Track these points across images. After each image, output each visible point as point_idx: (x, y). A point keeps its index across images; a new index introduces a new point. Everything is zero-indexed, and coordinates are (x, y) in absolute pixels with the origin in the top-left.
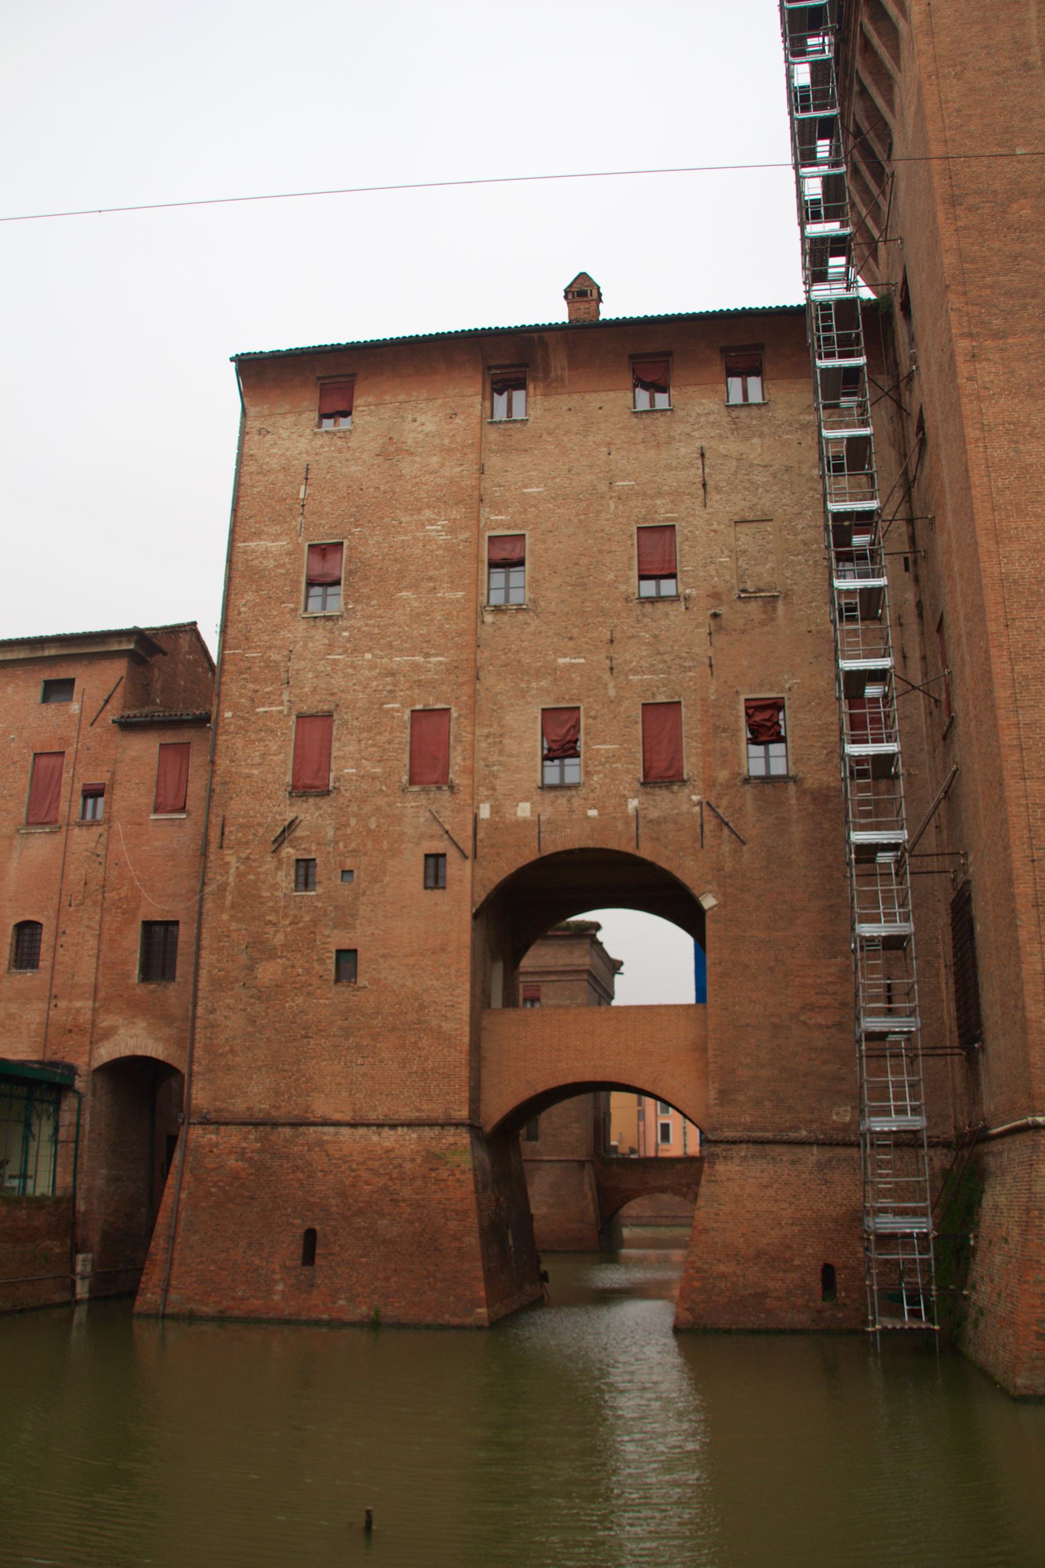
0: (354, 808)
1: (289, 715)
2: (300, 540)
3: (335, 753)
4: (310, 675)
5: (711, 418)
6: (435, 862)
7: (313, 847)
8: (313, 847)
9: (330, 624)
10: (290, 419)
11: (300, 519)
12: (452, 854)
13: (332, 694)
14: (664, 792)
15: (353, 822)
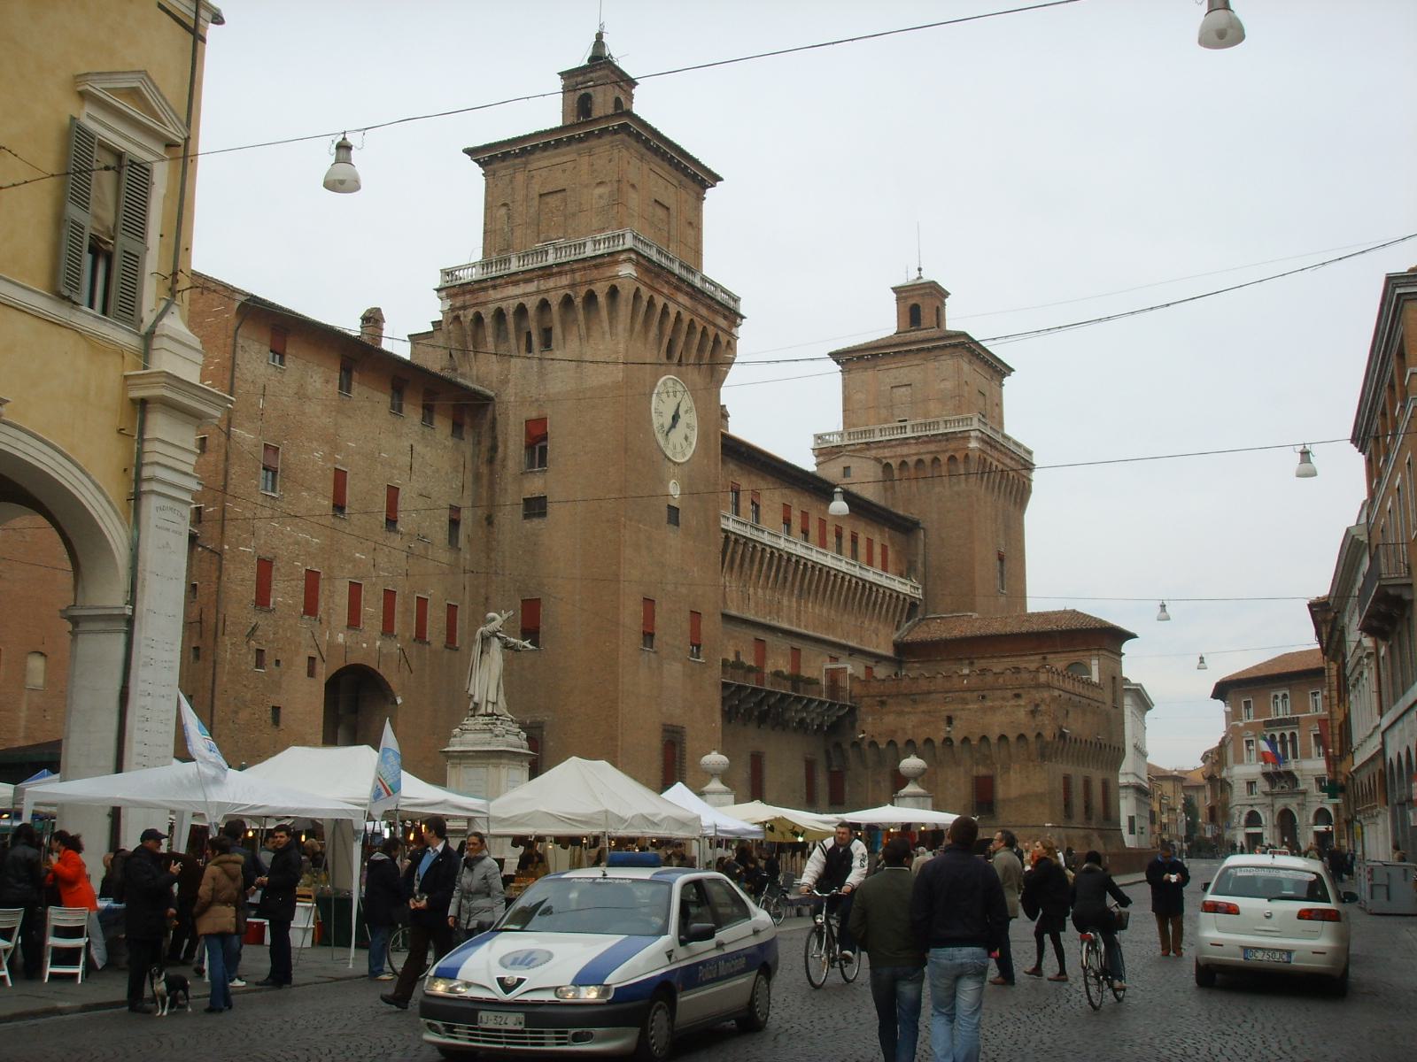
0: (281, 623)
1: (254, 556)
2: (260, 438)
3: (274, 587)
4: (264, 533)
5: (416, 428)
6: (312, 659)
7: (264, 643)
8: (264, 643)
9: (273, 501)
10: (256, 346)
11: (260, 422)
12: (318, 657)
13: (273, 548)
14: (388, 639)
15: (280, 631)
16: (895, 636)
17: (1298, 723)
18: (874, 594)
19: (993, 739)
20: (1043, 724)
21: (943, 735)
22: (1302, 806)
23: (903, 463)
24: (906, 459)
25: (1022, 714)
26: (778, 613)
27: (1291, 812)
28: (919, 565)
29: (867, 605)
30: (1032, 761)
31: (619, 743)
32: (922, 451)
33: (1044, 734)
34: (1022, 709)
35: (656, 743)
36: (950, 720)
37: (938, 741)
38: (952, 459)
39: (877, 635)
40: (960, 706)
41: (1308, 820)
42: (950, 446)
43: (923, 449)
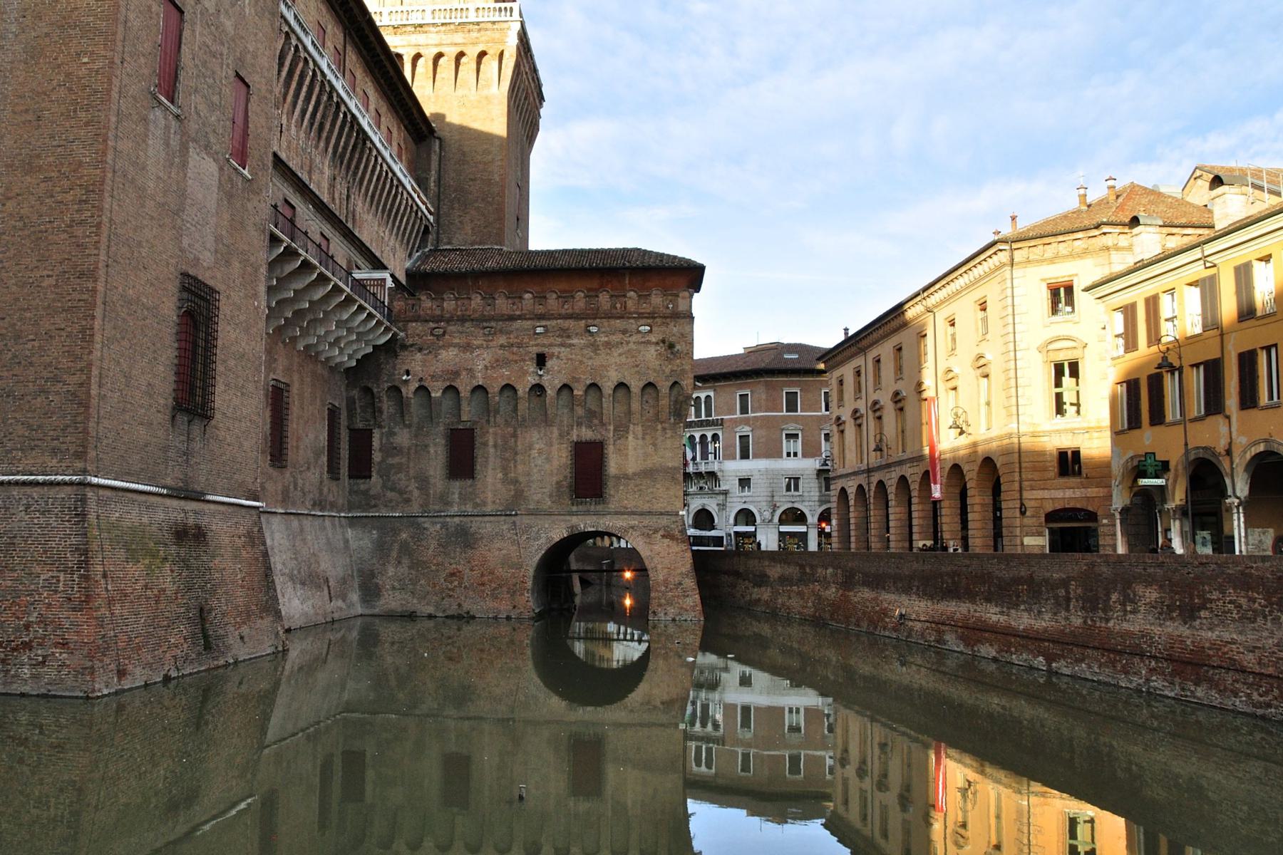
16: (408, 264)
17: (722, 425)
18: (399, 196)
19: (608, 387)
20: (683, 370)
21: (532, 380)
22: (722, 507)
23: (417, 57)
24: (422, 52)
25: (651, 354)
26: (310, 173)
27: (710, 513)
28: (432, 184)
29: (390, 211)
30: (662, 423)
31: (100, 287)
32: (444, 42)
33: (684, 383)
34: (652, 349)
35: (169, 308)
36: (541, 360)
37: (522, 390)
38: (482, 54)
39: (394, 255)
40: (559, 340)
41: (727, 520)
42: (483, 38)
43: (447, 38)
